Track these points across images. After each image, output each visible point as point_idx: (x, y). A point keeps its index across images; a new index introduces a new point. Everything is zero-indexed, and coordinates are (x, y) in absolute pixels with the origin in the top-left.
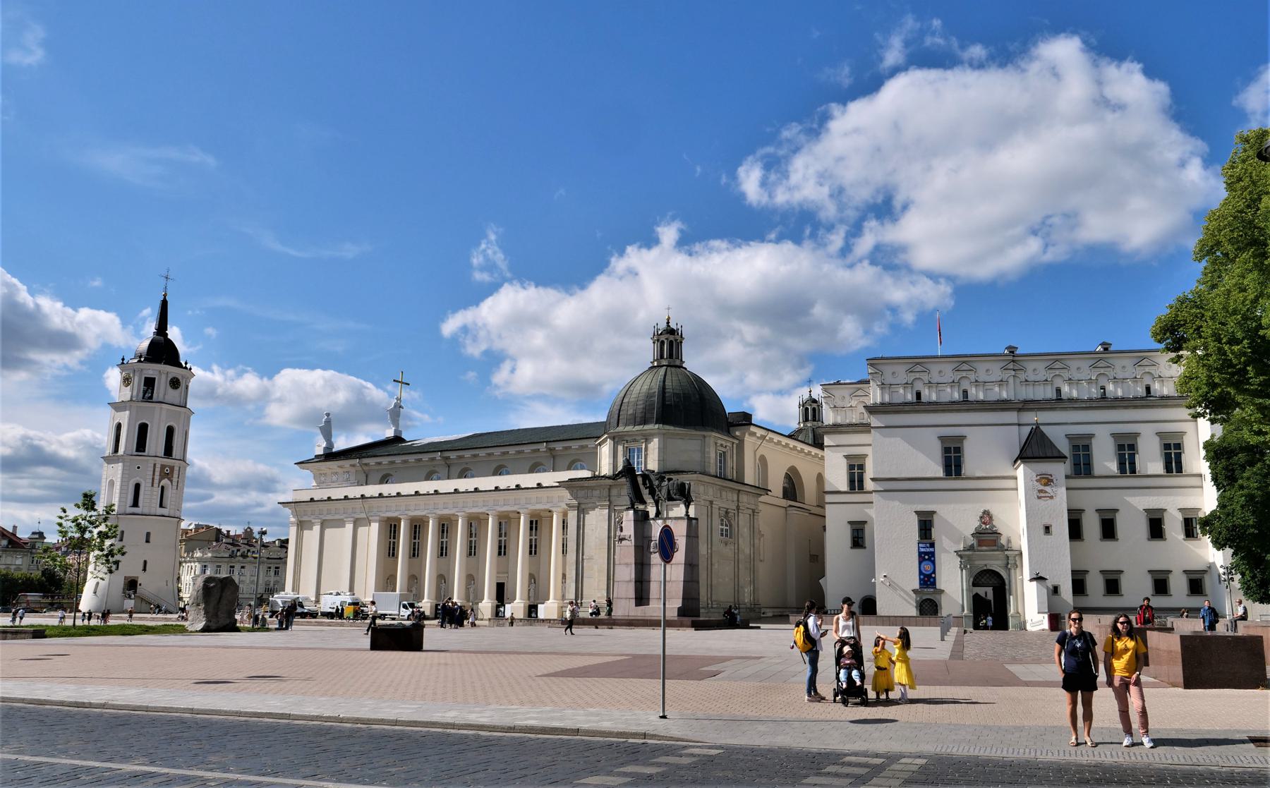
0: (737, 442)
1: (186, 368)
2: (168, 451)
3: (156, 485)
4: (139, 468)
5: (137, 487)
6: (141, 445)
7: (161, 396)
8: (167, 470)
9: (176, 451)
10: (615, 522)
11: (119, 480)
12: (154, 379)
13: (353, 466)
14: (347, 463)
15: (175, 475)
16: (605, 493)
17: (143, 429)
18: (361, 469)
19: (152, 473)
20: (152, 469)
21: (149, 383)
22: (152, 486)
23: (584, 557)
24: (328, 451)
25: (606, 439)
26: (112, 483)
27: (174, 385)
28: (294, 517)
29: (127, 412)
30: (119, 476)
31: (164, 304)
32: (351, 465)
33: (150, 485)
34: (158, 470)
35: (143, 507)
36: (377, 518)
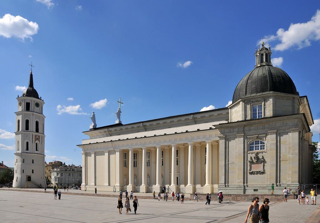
2: (37, 130)
3: (34, 142)
4: (27, 136)
5: (27, 143)
6: (27, 128)
7: (33, 109)
10: (247, 144)
11: (21, 140)
13: (105, 132)
14: (102, 131)
15: (41, 139)
16: (241, 129)
18: (108, 133)
23: (229, 163)
25: (240, 102)
28: (83, 151)
29: (21, 116)
30: (21, 139)
32: (104, 132)
36: (119, 150)
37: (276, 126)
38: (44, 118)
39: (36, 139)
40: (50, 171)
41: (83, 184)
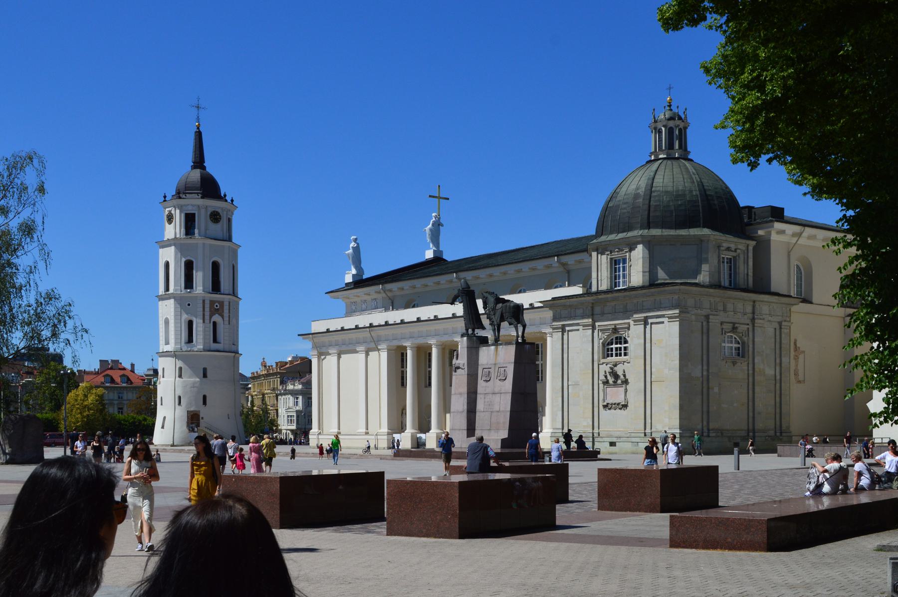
0: (754, 243)
1: (226, 201)
2: (216, 287)
3: (207, 321)
8: (217, 306)
9: (225, 284)
12: (194, 214)
19: (202, 309)
20: (201, 305)
22: (204, 322)
24: (358, 278)
26: (167, 322)
27: (215, 219)
30: (173, 314)
31: (199, 135)
34: (207, 306)
37: (644, 308)
38: (234, 253)
39: (213, 312)
40: (274, 389)
41: (315, 429)
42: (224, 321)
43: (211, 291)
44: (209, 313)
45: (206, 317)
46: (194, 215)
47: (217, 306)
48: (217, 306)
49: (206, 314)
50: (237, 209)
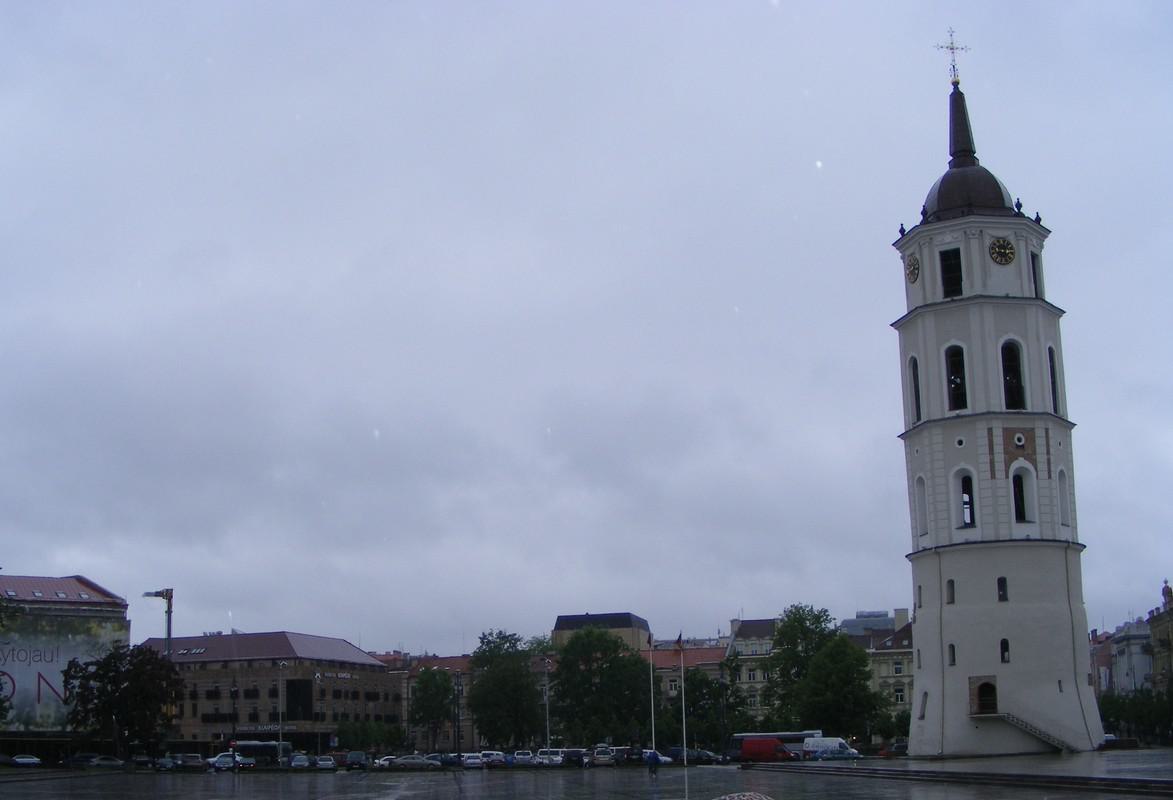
1: (1020, 215)
2: (1015, 396)
3: (1000, 474)
4: (960, 443)
6: (958, 398)
9: (1035, 396)
15: (1041, 449)
17: (955, 358)
20: (986, 441)
21: (951, 262)
22: (993, 476)
27: (1000, 254)
31: (957, 101)
33: (989, 475)
34: (998, 440)
35: (982, 524)
42: (1036, 469)
43: (1004, 409)
44: (1003, 456)
45: (996, 465)
46: (956, 252)
47: (1019, 440)
48: (1019, 440)
49: (996, 459)
50: (1050, 236)
